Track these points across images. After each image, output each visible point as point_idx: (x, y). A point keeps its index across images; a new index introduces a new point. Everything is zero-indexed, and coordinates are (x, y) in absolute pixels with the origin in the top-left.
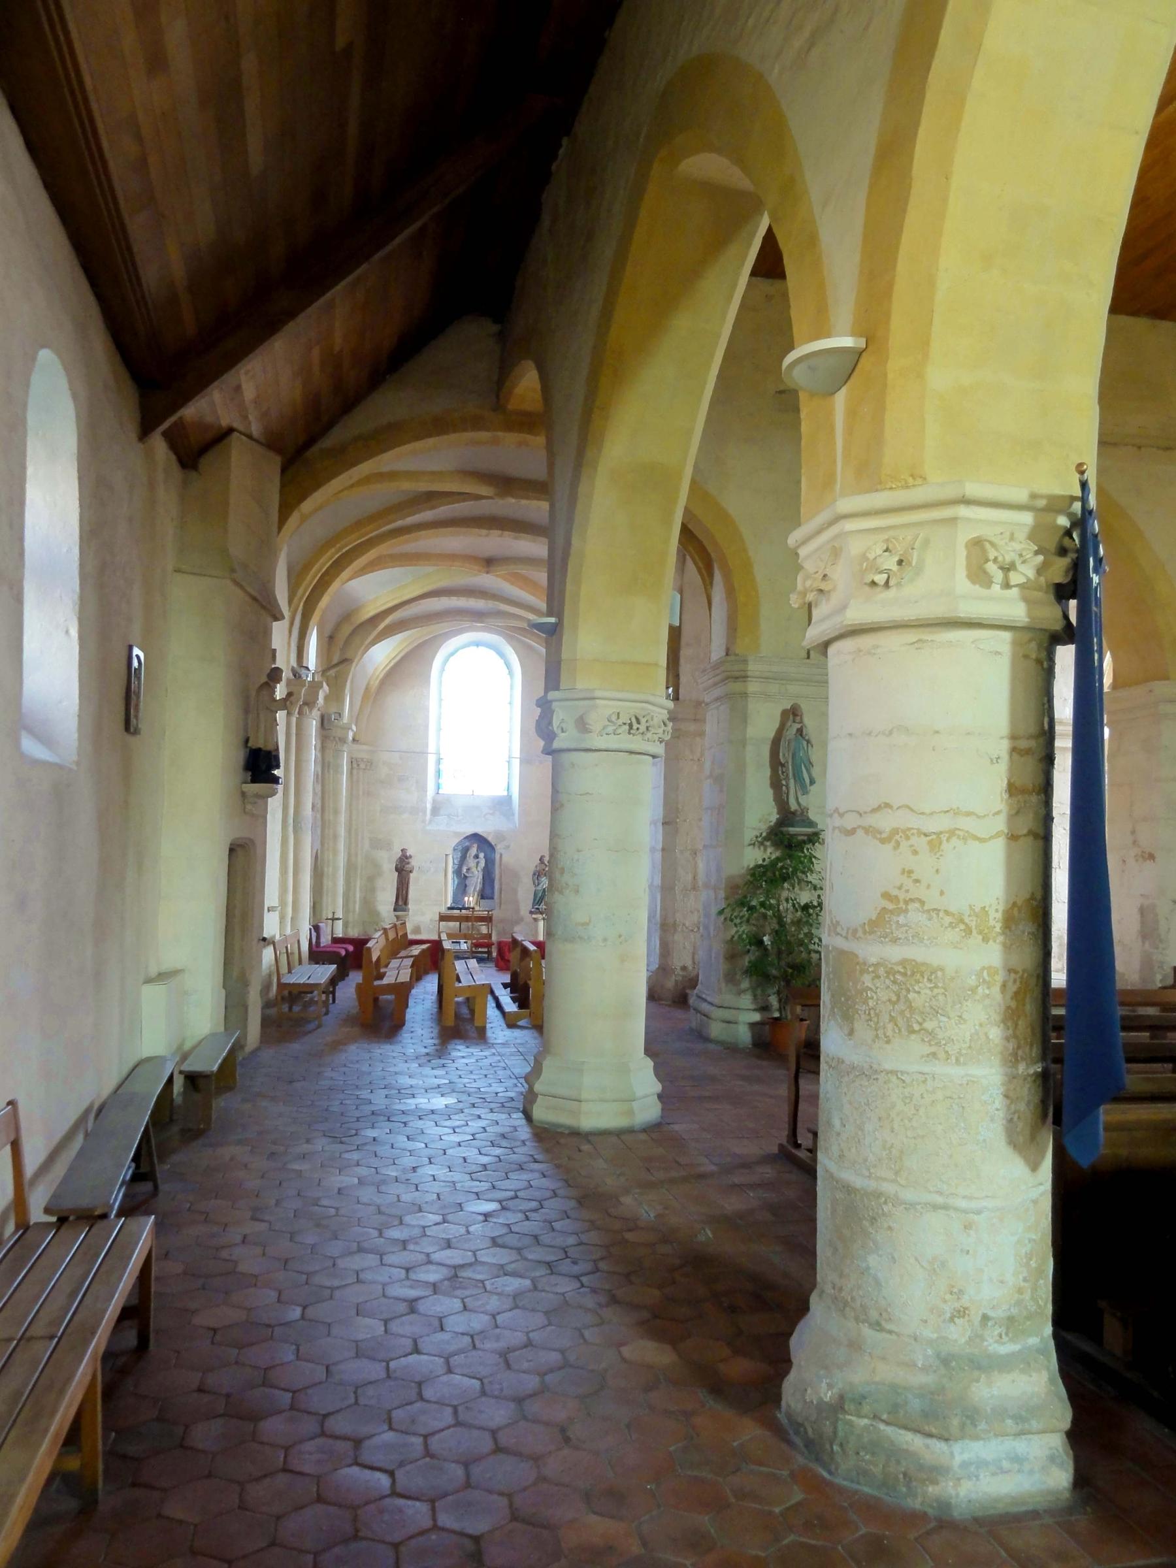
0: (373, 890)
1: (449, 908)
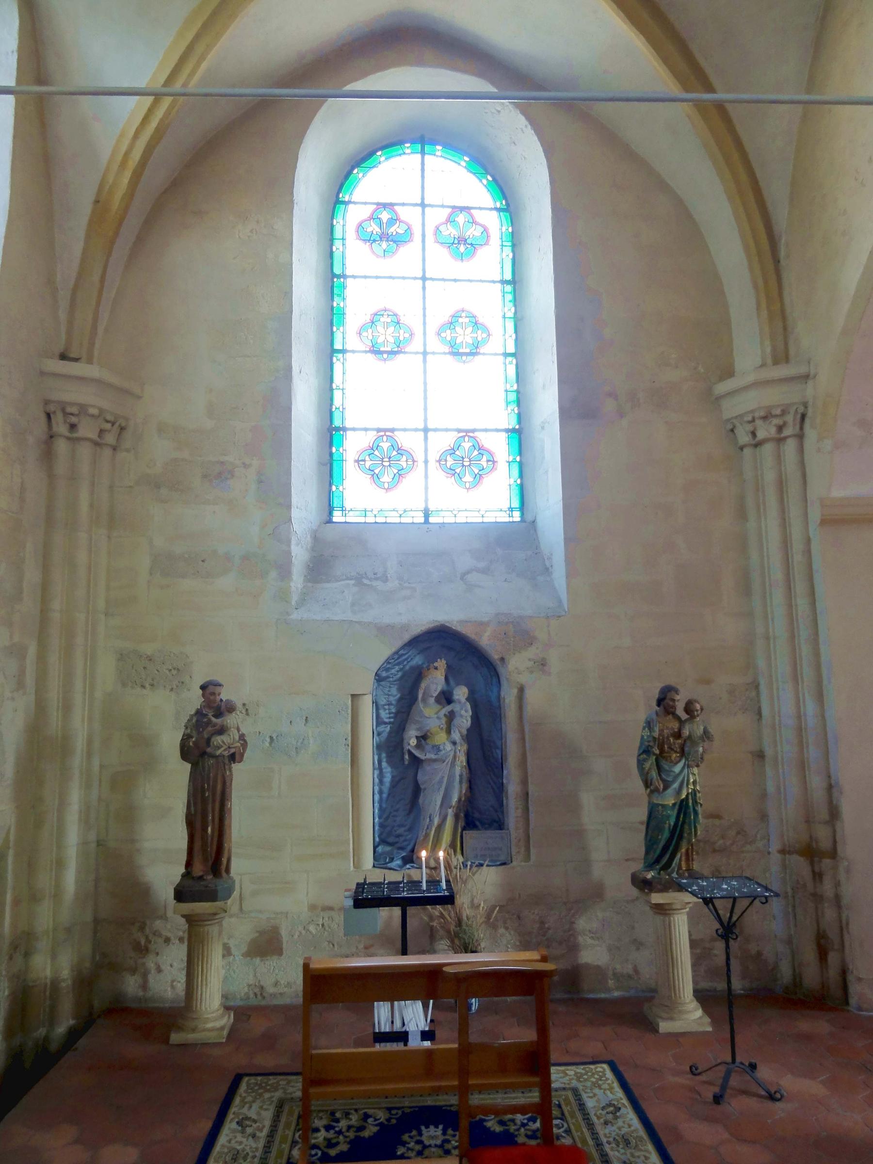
0: (128, 816)
1: (366, 898)
